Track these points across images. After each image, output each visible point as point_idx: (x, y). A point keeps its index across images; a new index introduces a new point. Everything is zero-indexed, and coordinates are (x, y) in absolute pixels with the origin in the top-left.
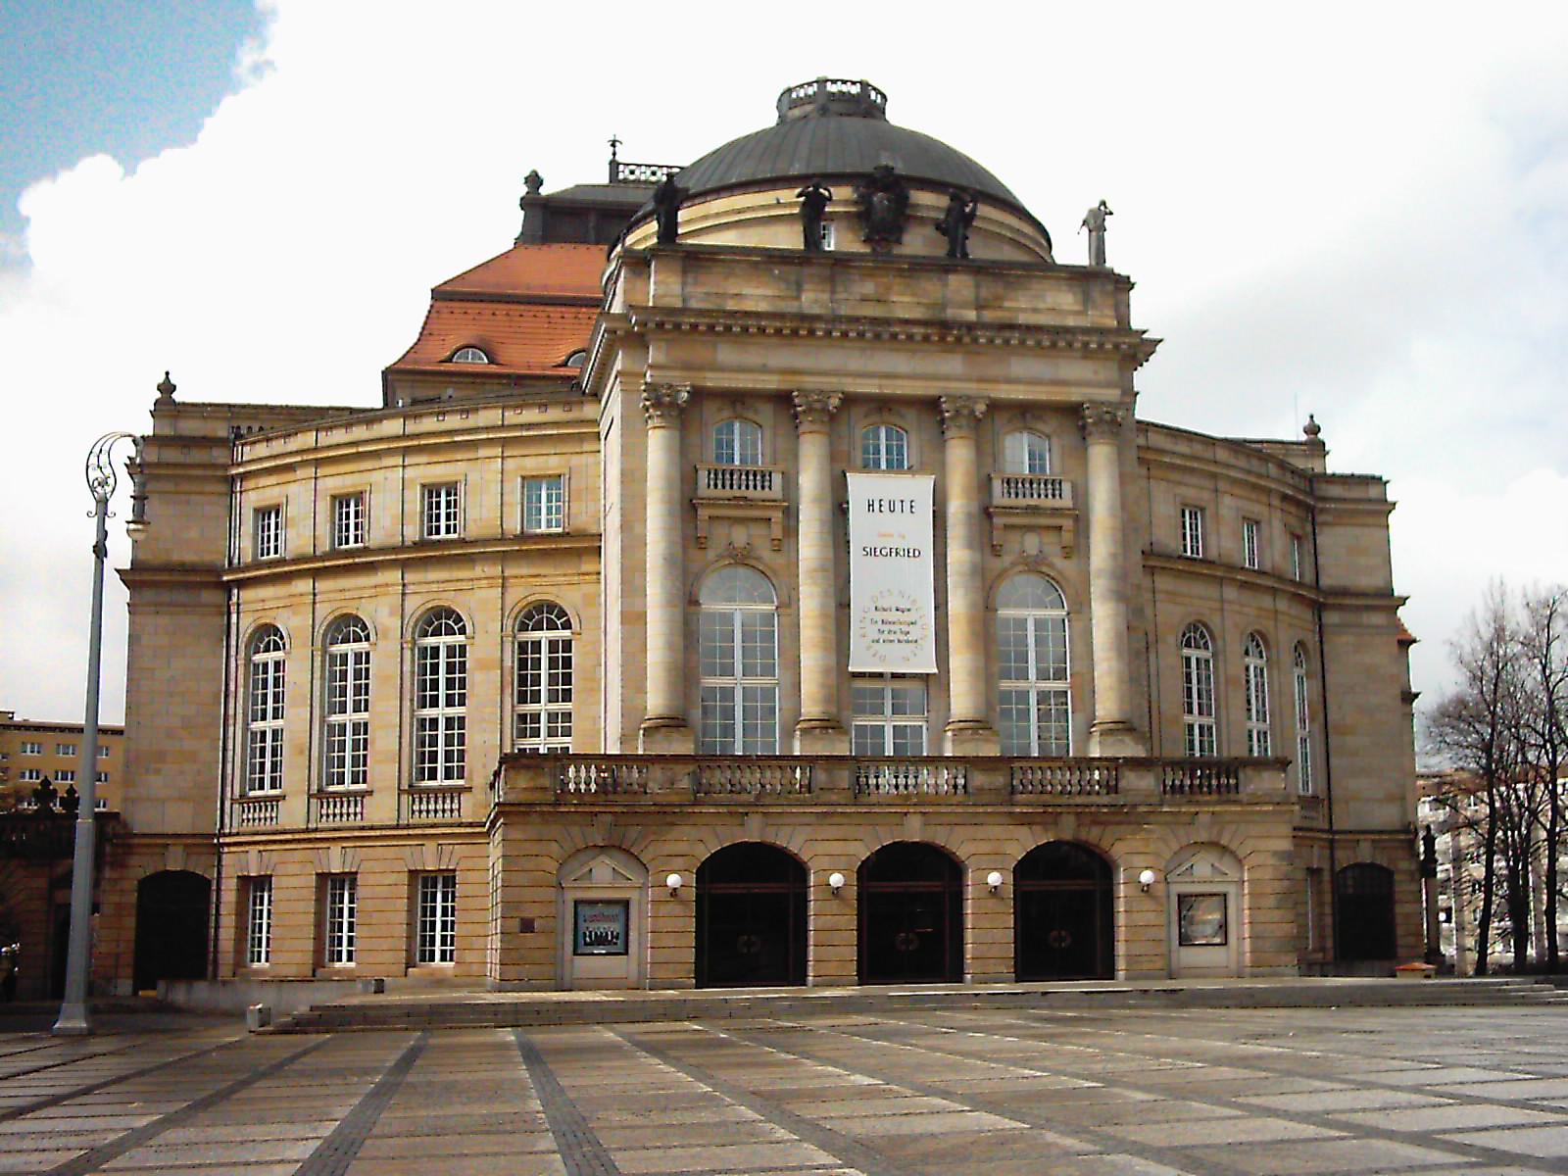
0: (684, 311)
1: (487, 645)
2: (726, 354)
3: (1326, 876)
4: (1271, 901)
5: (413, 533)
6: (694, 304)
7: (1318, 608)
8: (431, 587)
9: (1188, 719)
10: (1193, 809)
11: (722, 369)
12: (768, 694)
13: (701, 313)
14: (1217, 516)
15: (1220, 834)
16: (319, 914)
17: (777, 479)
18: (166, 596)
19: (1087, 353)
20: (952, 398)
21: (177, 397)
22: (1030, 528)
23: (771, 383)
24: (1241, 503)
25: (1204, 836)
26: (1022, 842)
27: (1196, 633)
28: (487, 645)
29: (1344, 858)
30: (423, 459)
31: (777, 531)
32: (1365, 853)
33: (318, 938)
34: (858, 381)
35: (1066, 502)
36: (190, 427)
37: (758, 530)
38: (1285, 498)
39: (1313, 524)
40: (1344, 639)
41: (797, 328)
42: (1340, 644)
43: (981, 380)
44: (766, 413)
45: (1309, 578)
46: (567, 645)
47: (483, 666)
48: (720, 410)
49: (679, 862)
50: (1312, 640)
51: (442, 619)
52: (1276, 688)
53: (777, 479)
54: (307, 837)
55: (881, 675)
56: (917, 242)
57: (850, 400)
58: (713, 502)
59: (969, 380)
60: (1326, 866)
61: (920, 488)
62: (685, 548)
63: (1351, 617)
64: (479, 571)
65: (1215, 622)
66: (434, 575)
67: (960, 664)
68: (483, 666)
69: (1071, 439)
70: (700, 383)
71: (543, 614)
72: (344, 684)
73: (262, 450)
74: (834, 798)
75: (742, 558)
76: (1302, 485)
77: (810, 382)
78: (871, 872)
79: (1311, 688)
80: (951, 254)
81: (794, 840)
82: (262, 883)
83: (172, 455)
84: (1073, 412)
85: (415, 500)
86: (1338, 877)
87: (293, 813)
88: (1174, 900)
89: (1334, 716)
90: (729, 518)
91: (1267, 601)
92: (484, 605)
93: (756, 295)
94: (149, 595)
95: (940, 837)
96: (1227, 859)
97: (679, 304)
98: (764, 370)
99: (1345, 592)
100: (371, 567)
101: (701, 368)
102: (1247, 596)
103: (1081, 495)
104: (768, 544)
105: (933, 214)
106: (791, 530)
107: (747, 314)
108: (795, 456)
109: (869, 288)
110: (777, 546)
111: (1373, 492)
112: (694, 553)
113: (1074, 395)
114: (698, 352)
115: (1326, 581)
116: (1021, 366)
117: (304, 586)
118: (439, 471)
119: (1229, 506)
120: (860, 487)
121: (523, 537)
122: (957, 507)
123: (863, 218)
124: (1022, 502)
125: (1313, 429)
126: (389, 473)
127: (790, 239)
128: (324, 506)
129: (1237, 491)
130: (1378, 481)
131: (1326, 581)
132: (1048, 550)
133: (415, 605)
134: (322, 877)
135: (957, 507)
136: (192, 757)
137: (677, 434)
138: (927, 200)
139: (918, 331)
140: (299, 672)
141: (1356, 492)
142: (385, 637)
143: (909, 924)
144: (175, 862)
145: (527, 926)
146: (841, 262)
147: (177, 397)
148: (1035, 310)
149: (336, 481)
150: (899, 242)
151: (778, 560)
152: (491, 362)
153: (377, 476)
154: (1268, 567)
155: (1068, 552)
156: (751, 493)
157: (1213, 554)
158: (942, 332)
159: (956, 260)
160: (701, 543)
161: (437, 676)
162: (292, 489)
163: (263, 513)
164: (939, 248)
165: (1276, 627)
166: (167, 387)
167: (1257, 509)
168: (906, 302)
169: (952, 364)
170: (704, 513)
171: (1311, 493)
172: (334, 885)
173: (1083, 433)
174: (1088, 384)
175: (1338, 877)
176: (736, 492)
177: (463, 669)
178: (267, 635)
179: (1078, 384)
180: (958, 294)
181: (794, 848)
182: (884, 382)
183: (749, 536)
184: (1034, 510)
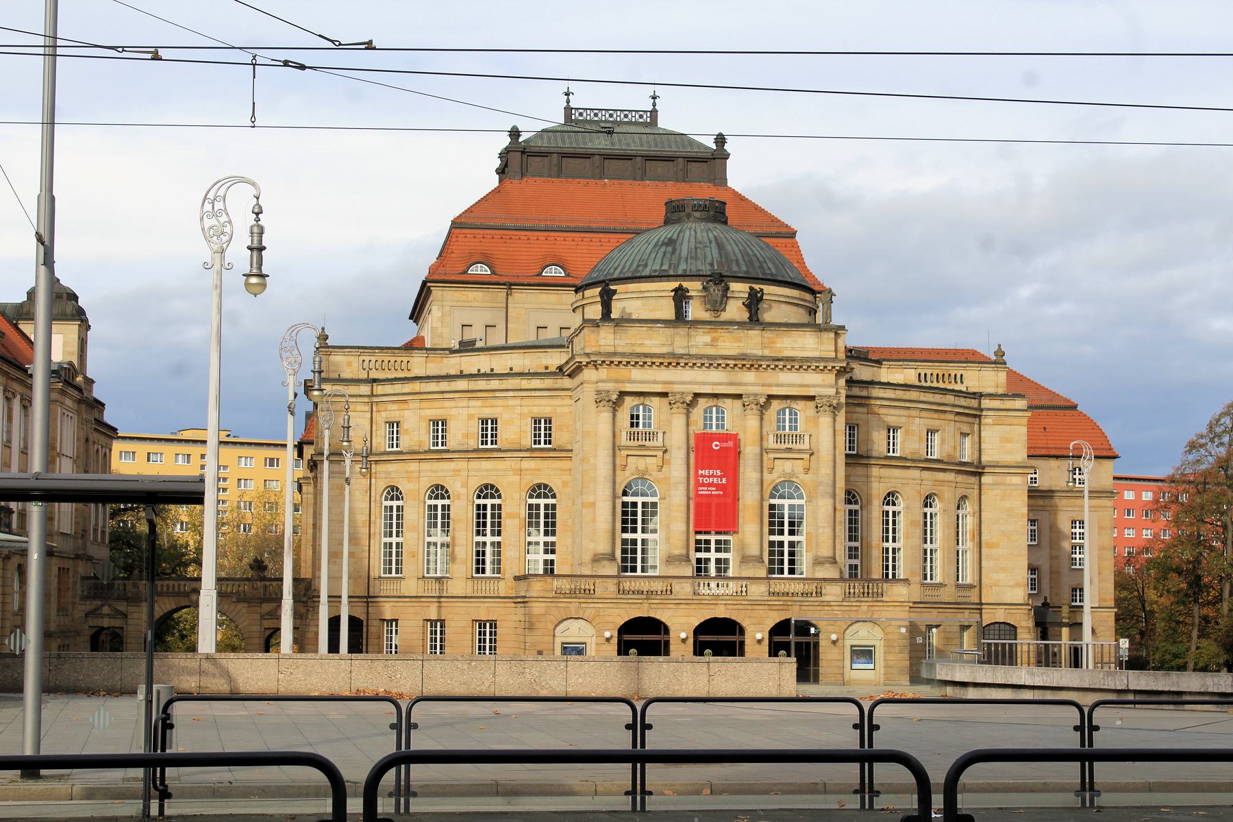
0: (615, 354)
1: (514, 505)
2: (636, 373)
4: (897, 649)
6: (620, 350)
8: (485, 471)
9: (885, 545)
11: (634, 382)
13: (623, 355)
20: (748, 395)
21: (330, 342)
23: (659, 388)
25: (863, 617)
26: (774, 618)
28: (514, 505)
29: (987, 619)
30: (479, 403)
32: (1000, 615)
35: (806, 446)
38: (958, 414)
40: (994, 492)
41: (673, 360)
43: (763, 385)
46: (554, 506)
47: (510, 516)
49: (611, 626)
51: (488, 490)
59: (757, 385)
63: (999, 479)
66: (486, 465)
68: (510, 516)
71: (542, 490)
77: (677, 388)
80: (750, 318)
85: (476, 428)
96: (877, 628)
97: (612, 349)
98: (655, 382)
101: (623, 382)
102: (926, 474)
105: (742, 295)
107: (646, 355)
108: (669, 422)
109: (708, 339)
114: (622, 372)
115: (984, 459)
118: (488, 412)
119: (919, 424)
124: (783, 446)
126: (460, 411)
127: (668, 312)
128: (424, 424)
129: (924, 414)
132: (796, 470)
138: (739, 289)
139: (731, 363)
142: (459, 498)
146: (697, 323)
147: (330, 342)
148: (793, 348)
150: (724, 310)
152: (493, 272)
153: (454, 411)
156: (648, 443)
159: (754, 320)
162: (407, 413)
164: (745, 316)
166: (323, 337)
169: (750, 376)
174: (819, 386)
176: (640, 443)
177: (500, 517)
178: (394, 492)
179: (814, 386)
180: (753, 342)
184: (789, 450)
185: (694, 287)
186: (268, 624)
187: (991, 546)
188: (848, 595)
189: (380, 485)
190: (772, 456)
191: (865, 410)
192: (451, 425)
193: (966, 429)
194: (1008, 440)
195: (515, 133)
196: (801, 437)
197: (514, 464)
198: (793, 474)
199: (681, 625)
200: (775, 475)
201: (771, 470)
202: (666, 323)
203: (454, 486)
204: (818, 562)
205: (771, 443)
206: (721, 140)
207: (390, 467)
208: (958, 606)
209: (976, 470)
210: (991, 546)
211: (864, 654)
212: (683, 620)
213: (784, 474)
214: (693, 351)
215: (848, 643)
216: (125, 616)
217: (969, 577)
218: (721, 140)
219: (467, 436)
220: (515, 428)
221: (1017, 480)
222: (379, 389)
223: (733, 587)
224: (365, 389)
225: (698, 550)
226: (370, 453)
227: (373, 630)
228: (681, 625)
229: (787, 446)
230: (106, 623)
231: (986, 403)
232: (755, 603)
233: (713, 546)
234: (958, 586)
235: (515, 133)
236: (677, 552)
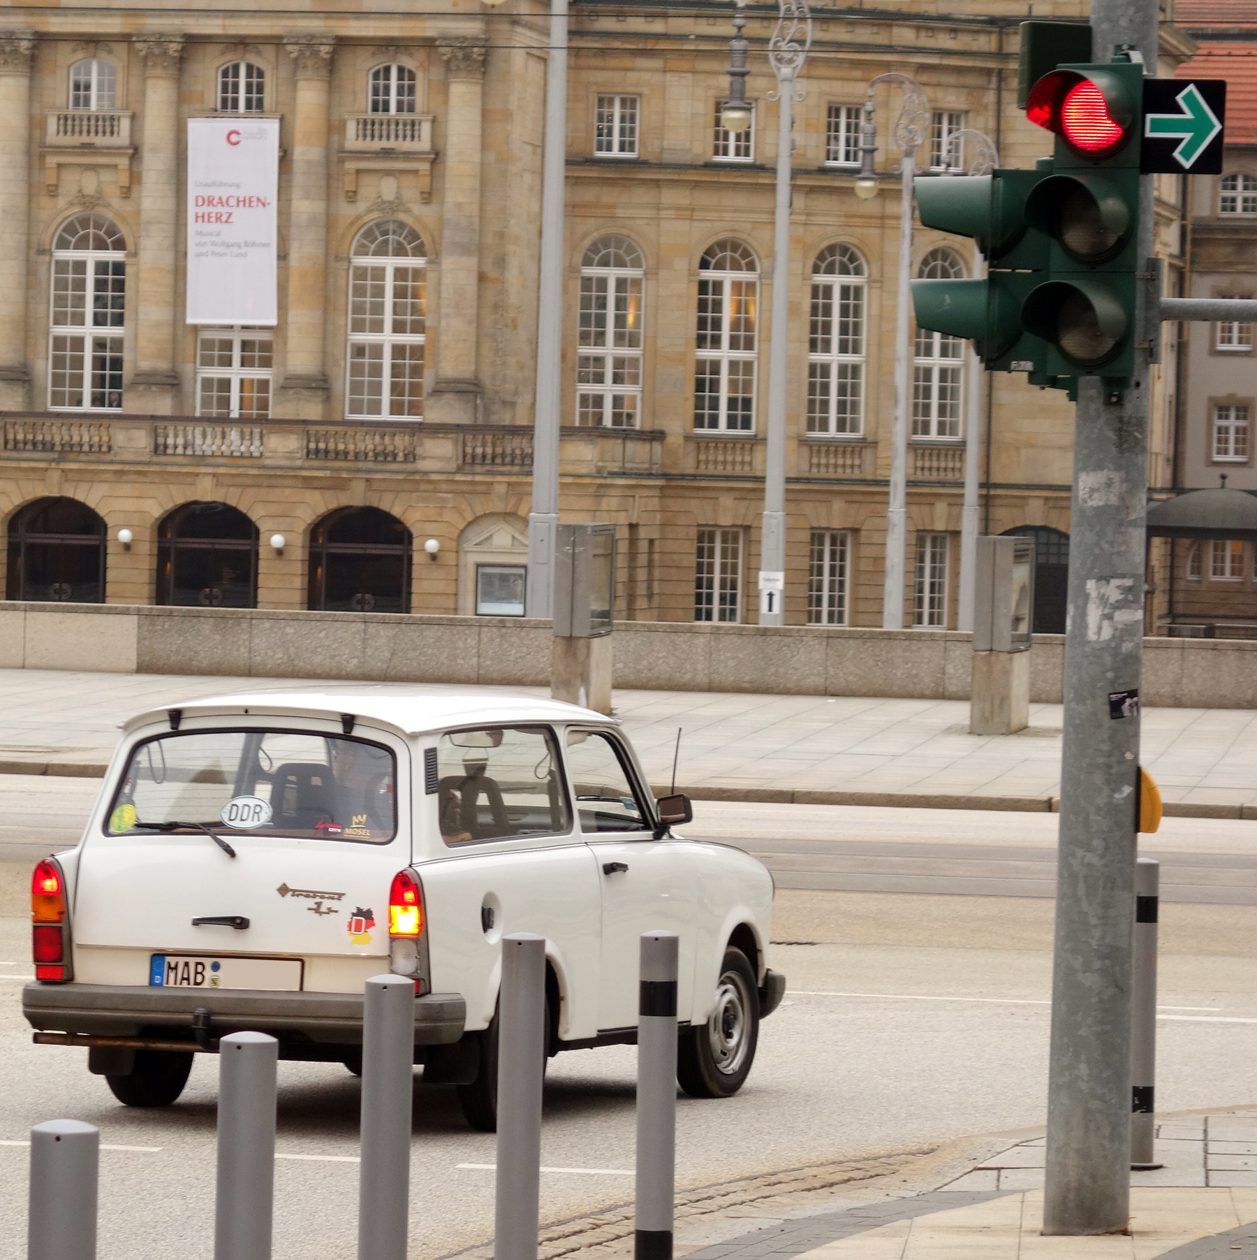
10: (488, 479)
15: (518, 504)
17: (125, 125)
22: (388, 173)
24: (826, 86)
25: (499, 507)
31: (124, 179)
34: (203, 21)
37: (106, 176)
38: (922, 68)
39: (999, 90)
43: (329, 14)
48: (74, 51)
52: (875, 311)
53: (125, 125)
55: (231, 327)
58: (59, 150)
61: (262, 135)
62: (31, 195)
67: (302, 317)
70: (44, 29)
74: (131, 457)
81: (92, 496)
88: (471, 571)
90: (80, 165)
95: (233, 497)
104: (118, 192)
106: (135, 178)
110: (127, 193)
112: (44, 201)
120: (204, 133)
122: (304, 153)
124: (377, 145)
135: (306, 153)
137: (24, 82)
155: (428, 197)
156: (99, 140)
160: (53, 191)
165: (882, 238)
170: (52, 161)
181: (91, 503)
182: (228, 22)
183: (99, 183)
184: (387, 154)
188: (468, 462)
190: (351, 166)
191: (658, 63)
193: (953, 100)
198: (397, 204)
199: (129, 518)
200: (361, 206)
205: (352, 139)
211: (501, 581)
212: (129, 505)
213: (381, 205)
215: (471, 559)
225: (207, 361)
228: (129, 518)
229: (385, 144)
232: (272, 477)
233: (236, 354)
236: (145, 365)
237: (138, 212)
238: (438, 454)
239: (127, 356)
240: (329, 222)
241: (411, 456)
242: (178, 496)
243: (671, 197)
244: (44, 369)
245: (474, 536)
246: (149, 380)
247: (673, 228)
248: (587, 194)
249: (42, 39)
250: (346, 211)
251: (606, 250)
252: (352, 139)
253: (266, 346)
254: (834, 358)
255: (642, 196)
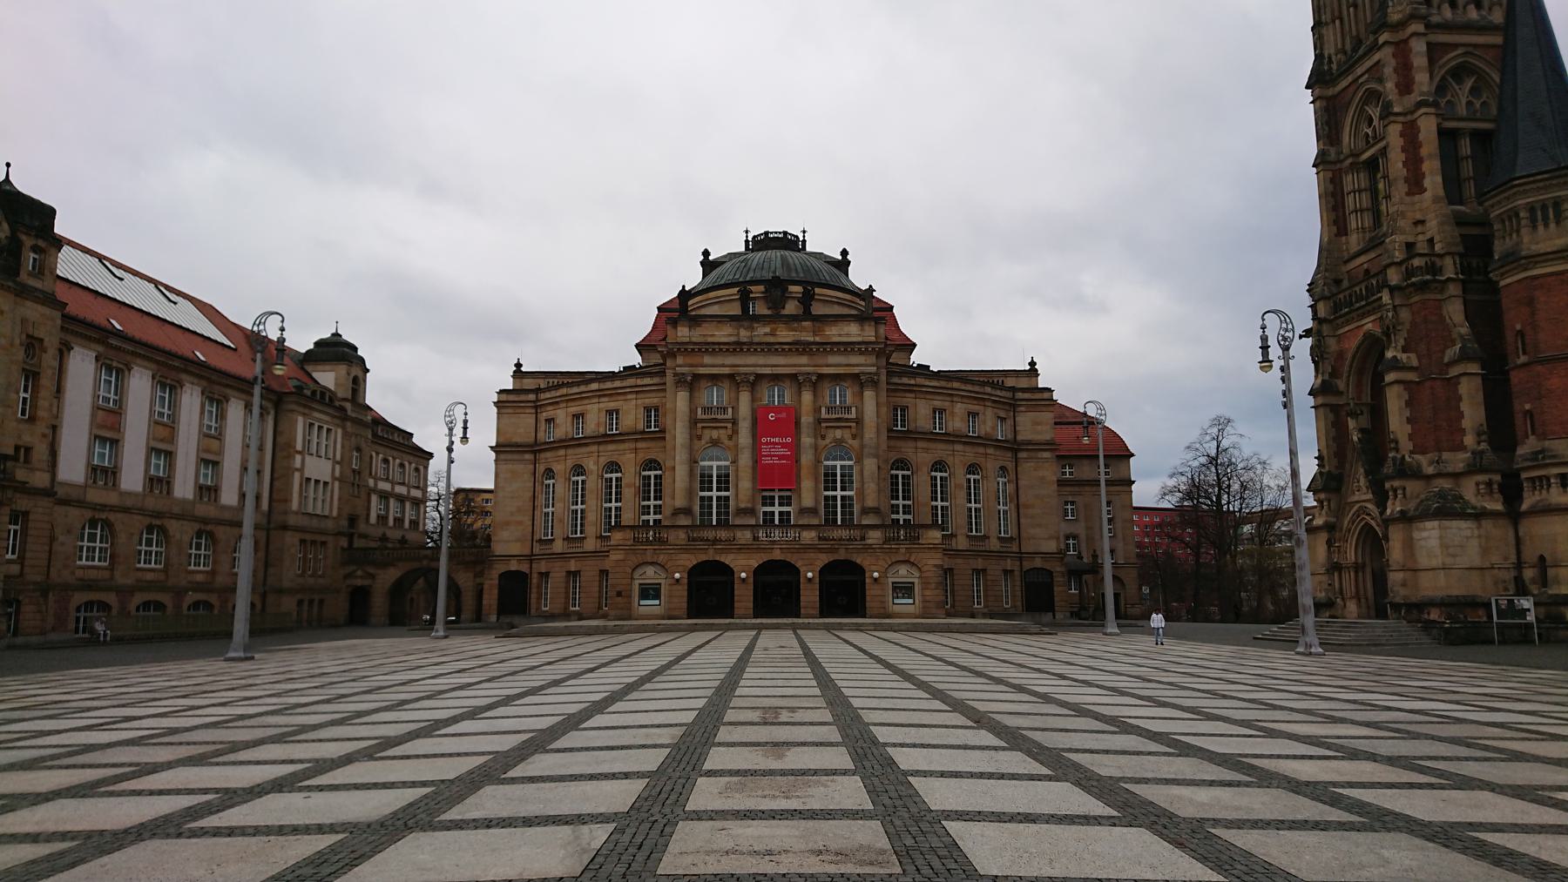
1: (630, 475)
2: (707, 360)
3: (1017, 573)
5: (602, 430)
7: (1015, 451)
8: (609, 452)
12: (727, 498)
14: (953, 414)
16: (567, 588)
18: (509, 456)
19: (861, 353)
23: (726, 371)
26: (823, 559)
27: (939, 465)
29: (1027, 565)
32: (1038, 563)
33: (567, 598)
35: (853, 416)
36: (529, 384)
37: (722, 431)
42: (1027, 467)
44: (726, 384)
45: (1010, 437)
47: (628, 486)
50: (1010, 465)
54: (562, 556)
56: (791, 308)
57: (759, 377)
58: (703, 421)
60: (1017, 568)
63: (1032, 454)
64: (626, 445)
65: (950, 460)
66: (611, 447)
68: (628, 486)
69: (857, 389)
71: (652, 464)
72: (578, 493)
73: (548, 395)
75: (715, 443)
76: (1009, 394)
78: (759, 572)
79: (1010, 488)
81: (727, 559)
82: (547, 574)
83: (512, 397)
84: (856, 377)
85: (603, 417)
86: (1026, 574)
87: (559, 546)
89: (1022, 500)
91: (981, 450)
92: (629, 460)
93: (723, 334)
94: (502, 456)
95: (789, 558)
99: (1029, 443)
100: (586, 445)
102: (968, 448)
103: (860, 412)
106: (735, 432)
109: (767, 330)
110: (730, 438)
111: (1046, 395)
113: (856, 370)
114: (696, 360)
115: (1019, 438)
116: (833, 359)
117: (562, 452)
118: (612, 405)
119: (960, 408)
121: (643, 432)
123: (767, 298)
125: (1032, 364)
127: (735, 310)
130: (1050, 390)
131: (1019, 438)
133: (603, 460)
134: (569, 573)
136: (520, 523)
138: (796, 289)
140: (561, 488)
141: (1038, 396)
143: (776, 596)
144: (514, 566)
145: (619, 594)
146: (757, 318)
149: (574, 409)
151: (731, 443)
154: (983, 433)
155: (854, 437)
157: (950, 429)
158: (799, 348)
159: (807, 315)
160: (700, 438)
161: (612, 490)
163: (549, 421)
166: (518, 365)
167: (976, 408)
168: (785, 335)
169: (804, 360)
171: (1013, 398)
172: (573, 575)
173: (862, 386)
175: (1026, 574)
178: (549, 473)
185: (757, 290)
186: (478, 580)
187: (1027, 507)
188: (887, 540)
189: (541, 468)
192: (588, 417)
193: (1002, 414)
194: (1038, 424)
195: (706, 253)
196: (849, 409)
197: (632, 445)
199: (743, 566)
200: (828, 441)
201: (823, 437)
202: (732, 318)
203: (590, 465)
204: (865, 511)
205: (824, 414)
206: (844, 253)
207: (548, 454)
208: (1000, 555)
209: (1014, 447)
210: (1027, 507)
211: (905, 590)
212: (744, 562)
214: (756, 340)
216: (373, 577)
217: (1012, 532)
218: (844, 253)
219: (598, 425)
220: (632, 415)
221: (1046, 455)
222: (542, 396)
223: (792, 534)
224: (532, 397)
225: (764, 504)
226: (536, 443)
227: (535, 581)
228: (743, 566)
230: (359, 582)
231: (1020, 395)
232: (807, 548)
234: (1000, 539)
235: (706, 253)
236: (743, 505)
237: (737, 446)
238: (875, 537)
239: (731, 503)
240: (816, 447)
241: (863, 538)
242: (765, 558)
243: (920, 444)
244: (697, 509)
245: (892, 571)
246: (741, 512)
247: (922, 456)
248: (892, 443)
249: (697, 377)
250: (822, 443)
251: (902, 464)
252: (824, 414)
253: (789, 498)
254: (973, 505)
255: (911, 444)
